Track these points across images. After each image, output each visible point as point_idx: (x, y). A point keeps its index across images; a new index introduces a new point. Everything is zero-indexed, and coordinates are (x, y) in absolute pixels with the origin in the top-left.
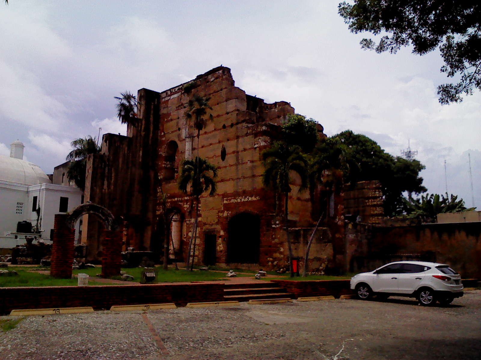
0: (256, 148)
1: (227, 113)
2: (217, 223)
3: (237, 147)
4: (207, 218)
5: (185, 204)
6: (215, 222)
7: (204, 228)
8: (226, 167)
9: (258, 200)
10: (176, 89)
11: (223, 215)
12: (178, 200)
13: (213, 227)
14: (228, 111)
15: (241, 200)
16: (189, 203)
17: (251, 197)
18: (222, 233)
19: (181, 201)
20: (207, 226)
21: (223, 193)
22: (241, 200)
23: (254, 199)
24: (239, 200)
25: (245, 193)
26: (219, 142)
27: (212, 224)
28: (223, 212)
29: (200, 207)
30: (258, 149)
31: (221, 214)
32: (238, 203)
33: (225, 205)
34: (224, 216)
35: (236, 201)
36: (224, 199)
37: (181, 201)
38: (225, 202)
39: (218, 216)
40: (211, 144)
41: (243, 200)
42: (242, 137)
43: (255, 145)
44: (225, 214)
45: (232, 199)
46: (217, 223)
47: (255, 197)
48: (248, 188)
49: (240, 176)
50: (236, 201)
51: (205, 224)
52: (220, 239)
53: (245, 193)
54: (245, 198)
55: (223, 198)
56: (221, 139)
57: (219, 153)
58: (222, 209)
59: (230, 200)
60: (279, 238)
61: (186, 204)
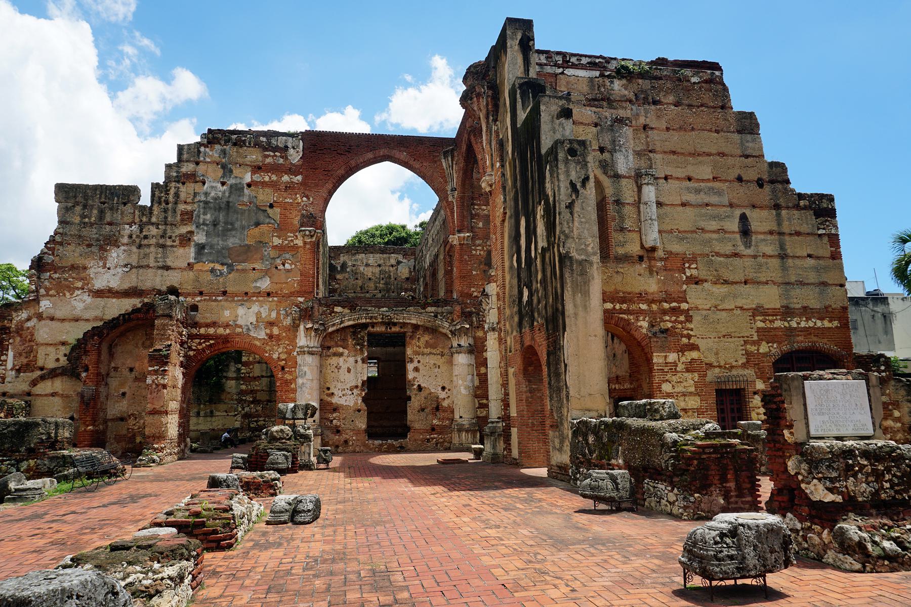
0: (820, 235)
1: (747, 157)
2: (744, 366)
3: (779, 224)
4: (717, 354)
5: (641, 318)
6: (740, 363)
7: (709, 373)
8: (755, 257)
9: (837, 327)
10: (584, 61)
11: (758, 350)
12: (614, 308)
13: (734, 372)
14: (747, 153)
15: (798, 324)
16: (647, 319)
17: (822, 319)
18: (760, 385)
19: (628, 312)
20: (717, 370)
21: (754, 306)
22: (798, 324)
23: (827, 324)
24: (794, 325)
25: (806, 312)
26: (731, 205)
27: (732, 367)
28: (757, 343)
29: (692, 330)
30: (826, 239)
31: (753, 348)
32: (791, 329)
33: (759, 330)
34: (761, 351)
35: (786, 324)
36: (757, 318)
37: (628, 312)
38: (760, 324)
39: (746, 350)
40: (707, 205)
41: (803, 324)
42: (788, 208)
43: (819, 229)
44: (764, 348)
45: (776, 319)
46: (744, 366)
47: (830, 321)
48: (814, 304)
49: (793, 279)
50: (786, 324)
51: (710, 365)
52: (756, 396)
53: (806, 312)
54: (807, 321)
55: (754, 316)
56: (734, 201)
57: (734, 225)
58: (755, 338)
59: (772, 321)
60: (889, 395)
61: (644, 320)
